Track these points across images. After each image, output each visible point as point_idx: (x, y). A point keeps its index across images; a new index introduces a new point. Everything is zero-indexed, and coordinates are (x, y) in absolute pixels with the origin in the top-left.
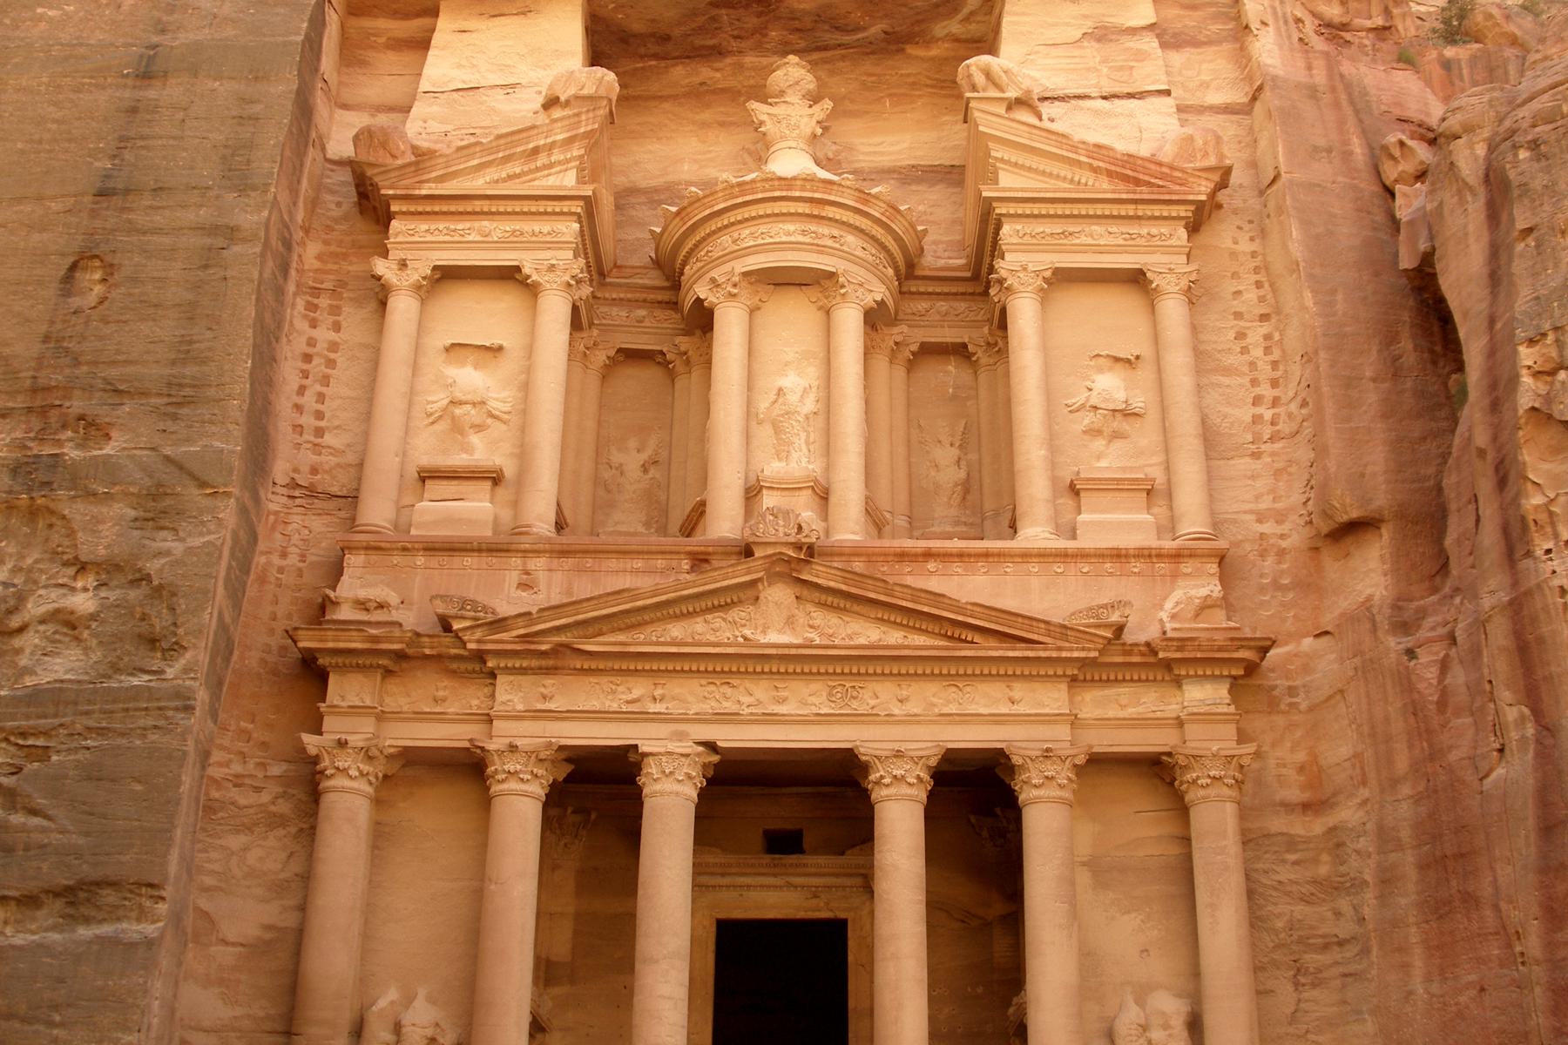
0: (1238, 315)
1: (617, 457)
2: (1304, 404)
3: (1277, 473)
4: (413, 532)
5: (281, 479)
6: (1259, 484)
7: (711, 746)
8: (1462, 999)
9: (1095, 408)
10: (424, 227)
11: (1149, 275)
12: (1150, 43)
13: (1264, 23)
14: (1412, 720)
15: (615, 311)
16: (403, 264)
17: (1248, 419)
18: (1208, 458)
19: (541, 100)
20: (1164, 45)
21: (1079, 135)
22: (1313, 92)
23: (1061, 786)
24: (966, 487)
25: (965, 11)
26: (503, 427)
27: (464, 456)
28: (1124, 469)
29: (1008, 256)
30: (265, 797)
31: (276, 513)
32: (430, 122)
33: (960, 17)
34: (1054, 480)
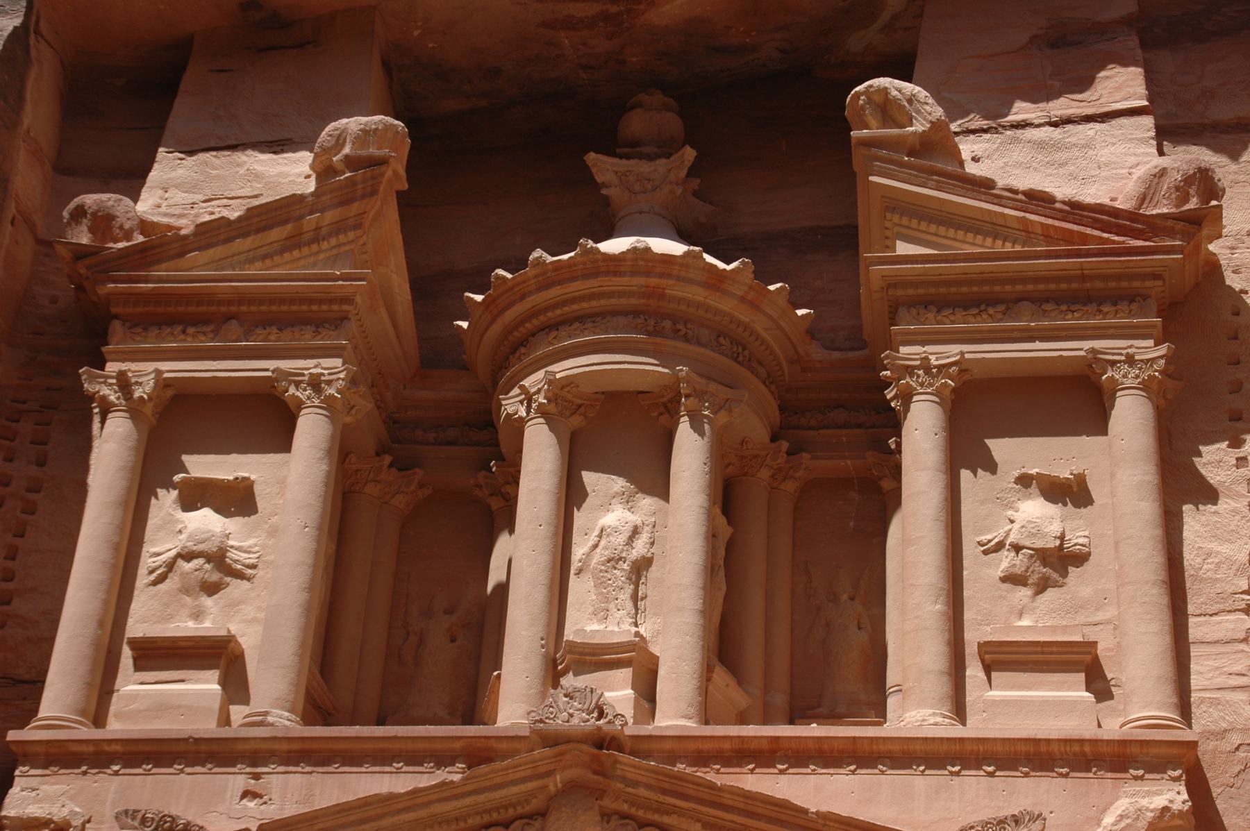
9: (1017, 548)
25: (886, 16)
27: (191, 624)
28: (1053, 629)
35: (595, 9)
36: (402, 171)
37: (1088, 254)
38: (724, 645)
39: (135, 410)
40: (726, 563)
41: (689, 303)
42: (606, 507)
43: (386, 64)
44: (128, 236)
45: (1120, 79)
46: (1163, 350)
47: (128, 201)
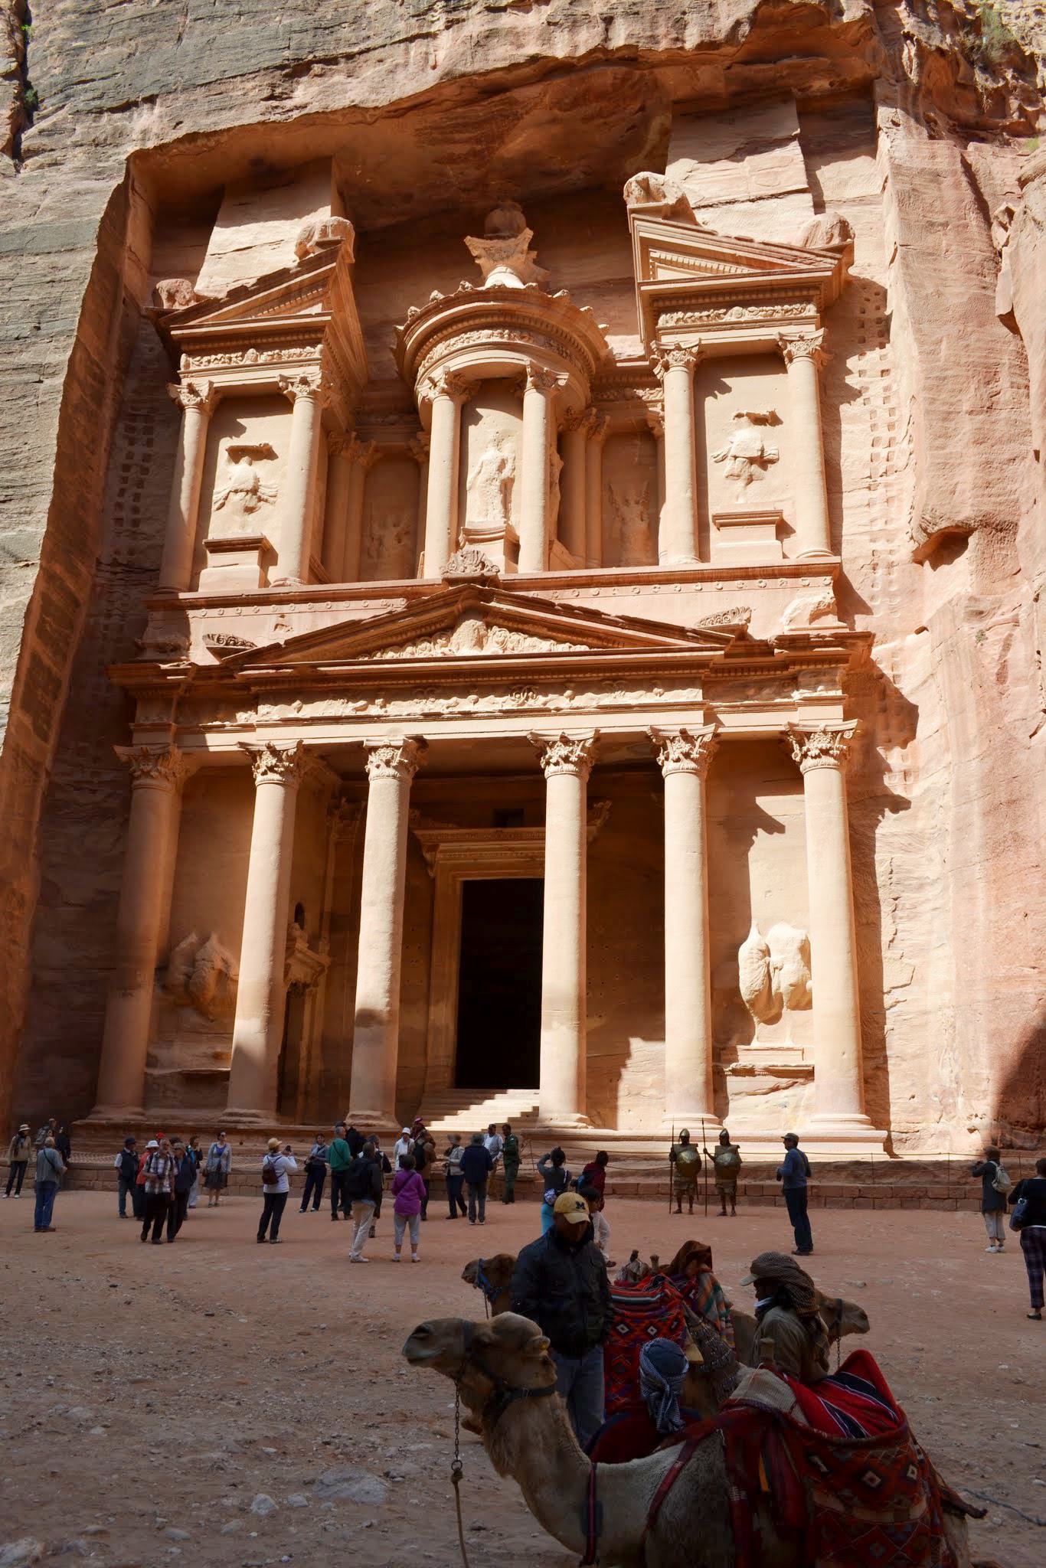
1: (377, 531)
5: (105, 560)
6: (876, 510)
7: (420, 740)
8: (1011, 923)
9: (736, 457)
10: (206, 358)
13: (896, 124)
14: (979, 691)
15: (373, 419)
16: (192, 390)
19: (294, 249)
21: (721, 233)
22: (936, 176)
25: (648, 147)
26: (271, 507)
28: (757, 504)
29: (665, 339)
30: (99, 797)
31: (102, 585)
32: (215, 278)
33: (644, 152)
35: (467, 148)
36: (351, 250)
37: (774, 274)
38: (560, 530)
39: (200, 406)
40: (560, 484)
41: (530, 319)
42: (484, 449)
43: (341, 194)
44: (187, 302)
45: (790, 173)
46: (821, 331)
47: (186, 283)
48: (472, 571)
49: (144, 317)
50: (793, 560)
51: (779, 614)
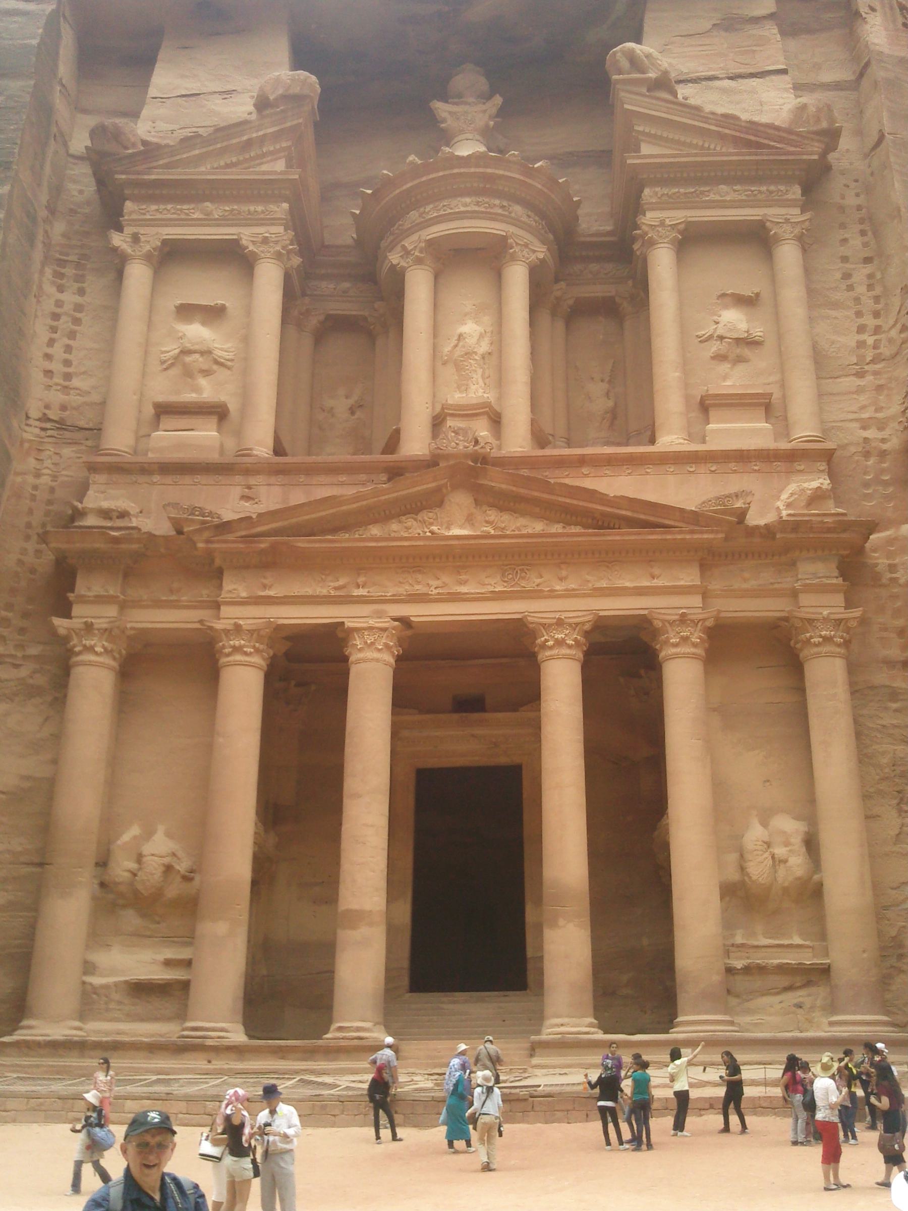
0: (845, 259)
2: (904, 329)
3: (879, 388)
4: (150, 455)
6: (863, 399)
9: (721, 338)
11: (768, 224)
12: (771, 31)
13: (873, 9)
16: (136, 238)
17: (854, 344)
18: (818, 378)
20: (783, 33)
23: (695, 645)
24: (613, 416)
34: (687, 398)
37: (761, 154)
48: (455, 444)
49: (73, 156)
50: (784, 445)
51: (777, 500)
